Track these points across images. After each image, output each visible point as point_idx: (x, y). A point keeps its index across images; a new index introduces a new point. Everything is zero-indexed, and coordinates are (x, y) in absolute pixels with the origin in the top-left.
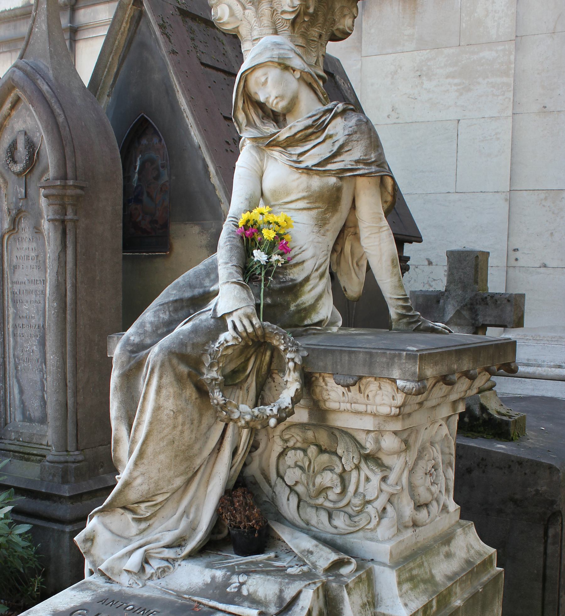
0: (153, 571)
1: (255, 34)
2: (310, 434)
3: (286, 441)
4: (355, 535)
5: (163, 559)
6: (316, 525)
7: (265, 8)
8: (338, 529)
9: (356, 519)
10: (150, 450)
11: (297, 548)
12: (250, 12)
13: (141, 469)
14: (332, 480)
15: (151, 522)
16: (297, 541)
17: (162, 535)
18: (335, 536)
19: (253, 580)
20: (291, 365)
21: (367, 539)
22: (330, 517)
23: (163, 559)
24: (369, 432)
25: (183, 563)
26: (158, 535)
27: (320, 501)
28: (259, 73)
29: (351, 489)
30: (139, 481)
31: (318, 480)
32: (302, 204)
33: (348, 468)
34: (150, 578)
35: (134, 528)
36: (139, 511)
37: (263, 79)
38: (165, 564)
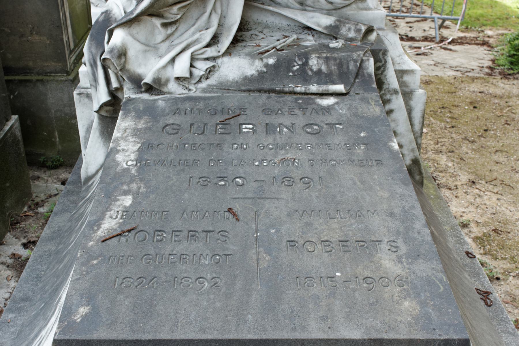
0: (202, 73)
4: (349, 8)
5: (207, 59)
6: (312, 4)
8: (334, 5)
11: (319, 25)
15: (177, 25)
16: (315, 20)
17: (201, 35)
18: (331, 11)
19: (312, 60)
21: (362, 9)
23: (207, 59)
25: (226, 59)
34: (200, 81)
35: (161, 34)
36: (167, 15)
38: (210, 64)
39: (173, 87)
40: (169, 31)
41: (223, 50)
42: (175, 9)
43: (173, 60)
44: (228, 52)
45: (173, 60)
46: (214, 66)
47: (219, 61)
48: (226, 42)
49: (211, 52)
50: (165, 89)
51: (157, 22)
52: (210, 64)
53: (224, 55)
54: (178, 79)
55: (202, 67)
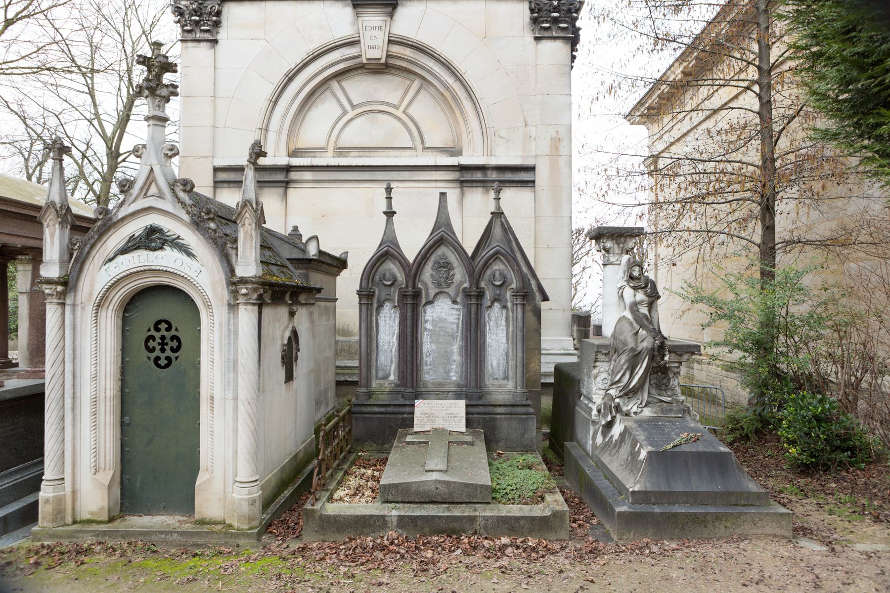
7: (621, 245)
12: (616, 246)
39: (632, 415)
41: (644, 405)
48: (644, 404)
49: (641, 406)
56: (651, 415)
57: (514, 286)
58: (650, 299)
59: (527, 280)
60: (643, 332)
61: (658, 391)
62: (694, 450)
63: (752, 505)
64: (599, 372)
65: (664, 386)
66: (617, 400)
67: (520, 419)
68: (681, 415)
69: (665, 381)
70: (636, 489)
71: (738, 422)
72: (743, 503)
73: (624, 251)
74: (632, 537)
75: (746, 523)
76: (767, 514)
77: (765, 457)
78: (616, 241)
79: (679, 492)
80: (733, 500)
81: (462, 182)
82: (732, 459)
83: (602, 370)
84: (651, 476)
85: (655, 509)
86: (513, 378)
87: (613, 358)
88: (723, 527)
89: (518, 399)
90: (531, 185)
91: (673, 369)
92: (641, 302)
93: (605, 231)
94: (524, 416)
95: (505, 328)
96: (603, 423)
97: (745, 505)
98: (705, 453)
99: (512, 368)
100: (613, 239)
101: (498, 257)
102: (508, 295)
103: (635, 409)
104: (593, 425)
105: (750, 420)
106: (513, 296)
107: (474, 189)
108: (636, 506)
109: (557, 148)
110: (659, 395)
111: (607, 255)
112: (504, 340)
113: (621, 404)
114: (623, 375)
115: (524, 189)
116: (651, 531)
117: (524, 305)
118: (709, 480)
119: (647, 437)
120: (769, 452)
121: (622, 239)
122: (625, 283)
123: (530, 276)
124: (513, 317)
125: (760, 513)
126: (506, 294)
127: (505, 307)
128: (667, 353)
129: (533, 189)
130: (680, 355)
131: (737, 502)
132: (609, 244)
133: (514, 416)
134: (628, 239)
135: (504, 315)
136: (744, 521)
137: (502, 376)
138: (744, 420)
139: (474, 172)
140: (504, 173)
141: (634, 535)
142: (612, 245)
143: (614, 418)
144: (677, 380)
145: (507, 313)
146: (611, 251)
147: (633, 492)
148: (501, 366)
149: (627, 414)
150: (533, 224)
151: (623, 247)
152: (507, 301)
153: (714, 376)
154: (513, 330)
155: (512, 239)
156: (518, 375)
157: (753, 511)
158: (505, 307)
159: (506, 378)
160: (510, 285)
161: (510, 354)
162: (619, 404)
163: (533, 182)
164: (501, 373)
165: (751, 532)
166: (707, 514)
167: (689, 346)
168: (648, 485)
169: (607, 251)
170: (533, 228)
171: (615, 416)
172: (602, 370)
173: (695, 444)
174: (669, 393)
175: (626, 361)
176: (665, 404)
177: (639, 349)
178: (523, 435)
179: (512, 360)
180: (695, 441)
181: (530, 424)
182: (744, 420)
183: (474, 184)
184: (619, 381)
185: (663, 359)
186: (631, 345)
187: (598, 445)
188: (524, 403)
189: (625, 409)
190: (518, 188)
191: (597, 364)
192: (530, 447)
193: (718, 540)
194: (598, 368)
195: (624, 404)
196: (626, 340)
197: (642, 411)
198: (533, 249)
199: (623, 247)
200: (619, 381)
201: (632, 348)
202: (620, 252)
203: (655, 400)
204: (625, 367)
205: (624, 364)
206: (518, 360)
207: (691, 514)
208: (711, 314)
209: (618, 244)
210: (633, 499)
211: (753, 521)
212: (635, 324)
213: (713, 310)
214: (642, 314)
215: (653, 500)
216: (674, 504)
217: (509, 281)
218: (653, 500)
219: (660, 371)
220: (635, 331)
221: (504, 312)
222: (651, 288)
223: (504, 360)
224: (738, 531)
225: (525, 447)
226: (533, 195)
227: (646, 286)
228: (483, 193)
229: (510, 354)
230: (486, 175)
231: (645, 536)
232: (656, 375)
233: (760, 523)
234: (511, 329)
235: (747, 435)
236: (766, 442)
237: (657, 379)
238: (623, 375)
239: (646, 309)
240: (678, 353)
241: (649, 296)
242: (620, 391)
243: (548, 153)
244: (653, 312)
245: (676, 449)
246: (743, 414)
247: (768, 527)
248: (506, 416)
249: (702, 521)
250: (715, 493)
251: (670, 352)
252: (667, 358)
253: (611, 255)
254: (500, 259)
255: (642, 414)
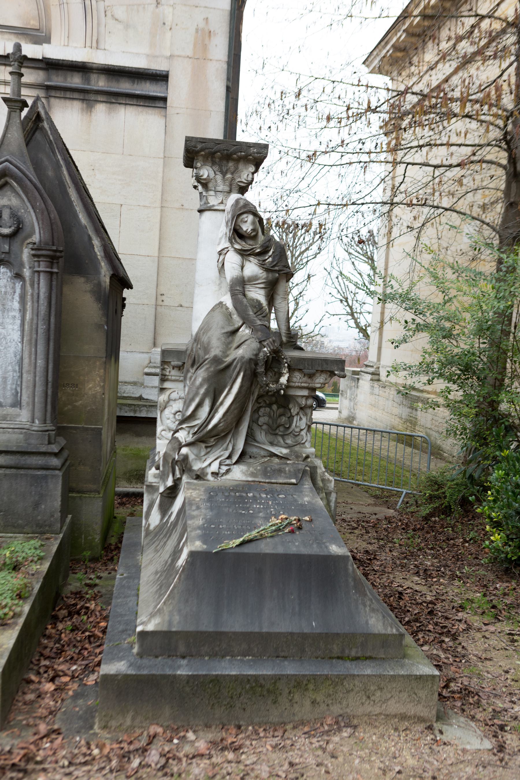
1: (220, 188)
2: (274, 399)
3: (260, 403)
7: (229, 176)
9: (297, 438)
10: (232, 408)
11: (281, 453)
12: (219, 177)
13: (225, 418)
14: (285, 421)
20: (286, 365)
22: (284, 440)
24: (303, 396)
25: (235, 466)
26: (222, 453)
27: (277, 431)
28: (245, 216)
29: (294, 424)
30: (221, 425)
31: (279, 421)
32: (262, 286)
33: (294, 414)
34: (222, 476)
37: (246, 219)
38: (227, 468)
39: (210, 477)
40: (209, 449)
41: (234, 461)
42: (212, 440)
43: (210, 465)
44: (236, 463)
45: (210, 465)
46: (229, 469)
47: (232, 467)
48: (235, 458)
49: (228, 462)
50: (206, 478)
51: (203, 445)
52: (227, 468)
53: (235, 464)
54: (212, 473)
55: (224, 469)
56: (244, 478)
57: (36, 238)
58: (270, 275)
59: (86, 238)
60: (245, 332)
61: (271, 438)
62: (280, 550)
63: (370, 658)
64: (169, 400)
65: (281, 429)
66: (184, 450)
67: (33, 477)
68: (294, 481)
69: (284, 419)
70: (150, 627)
71: (440, 486)
72: (353, 654)
73: (235, 188)
74: (128, 722)
75: (352, 694)
76: (393, 678)
77: (465, 541)
78: (220, 167)
79: (235, 633)
80: (336, 650)
81: (48, 88)
82: (346, 569)
83: (174, 396)
84: (187, 601)
85: (179, 667)
86: (28, 404)
87: (189, 375)
88: (307, 703)
89: (33, 441)
90: (161, 104)
91: (299, 400)
92: (253, 280)
93: (199, 146)
94: (39, 473)
95: (17, 314)
96: (162, 489)
97: (357, 658)
98: (299, 557)
99: (28, 387)
100: (213, 163)
101: (6, 184)
102: (26, 254)
103: (215, 467)
104: (149, 492)
105: (457, 484)
106: (34, 256)
107: (68, 103)
108: (145, 661)
109: (205, 48)
110: (272, 444)
111: (204, 193)
112: (16, 336)
113: (192, 457)
114: (199, 405)
115: (150, 111)
116: (167, 711)
117: (51, 273)
118: (297, 609)
119: (209, 522)
120: (472, 534)
121: (231, 164)
122: (228, 244)
123: (91, 232)
124: (32, 295)
125: (380, 676)
126: (22, 252)
127: (18, 276)
128: (285, 371)
129: (164, 110)
130: (311, 376)
131: (343, 651)
132: (206, 172)
133: (22, 472)
134: (241, 166)
135: (18, 291)
136: (348, 692)
137: (9, 401)
138: (449, 484)
139: (69, 74)
140: (118, 81)
141: (133, 719)
142: (212, 175)
143: (177, 483)
144: (304, 420)
145: (23, 287)
146: (210, 185)
147: (143, 634)
148: (9, 382)
149: (200, 476)
150: (161, 169)
151: (233, 179)
152: (22, 265)
153: (440, 421)
154: (32, 319)
155: (62, 162)
156: (36, 400)
157: (368, 672)
158: (18, 276)
159: (17, 403)
160: (30, 236)
161: (26, 361)
162: (186, 457)
163: (164, 99)
164: (8, 394)
165: (360, 711)
166: (277, 679)
167: (326, 361)
168: (177, 618)
169: (204, 183)
170: (161, 175)
171: (180, 479)
172: (174, 396)
173: (289, 538)
174: (289, 441)
175: (204, 380)
176: (277, 460)
177: (229, 360)
178: (36, 505)
179: (28, 372)
180: (292, 532)
181: (51, 486)
182: (449, 484)
183: (68, 94)
184: (193, 416)
185: (277, 381)
186: (216, 350)
187: (152, 528)
188: (43, 449)
189: (197, 466)
190: (140, 109)
191: (167, 385)
192: (50, 526)
193: (294, 728)
194: (168, 393)
195: (198, 458)
196: (209, 343)
197: (228, 471)
198: (159, 210)
199: (233, 179)
200: (193, 416)
201: (215, 357)
202: (227, 189)
203: (263, 453)
204: (202, 391)
205: (201, 385)
206: (38, 374)
207: (248, 679)
208: (406, 322)
209: (224, 174)
210: (141, 646)
211: (365, 690)
212: (235, 317)
213: (409, 316)
214: (253, 300)
215: (182, 648)
216: (223, 657)
217: (27, 230)
218: (182, 648)
219: (276, 402)
220: (230, 329)
221: (18, 286)
222: (273, 256)
223: (14, 371)
224: (336, 709)
225: (39, 525)
226: (164, 121)
227: (264, 252)
228: (82, 109)
229: (26, 361)
230: (88, 81)
231: (154, 720)
232: (268, 409)
233: (378, 693)
234: (28, 316)
235: (449, 507)
236: (473, 517)
237: (270, 417)
238: (199, 405)
239: (262, 292)
240: (306, 371)
241: (267, 270)
242: (195, 434)
243: (190, 53)
244: (279, 301)
245: (247, 549)
246: (448, 475)
247: (392, 702)
248: (8, 471)
249: (268, 691)
250: (304, 636)
251: (291, 369)
252: (284, 380)
253: (212, 193)
254: (12, 187)
255: (228, 477)
